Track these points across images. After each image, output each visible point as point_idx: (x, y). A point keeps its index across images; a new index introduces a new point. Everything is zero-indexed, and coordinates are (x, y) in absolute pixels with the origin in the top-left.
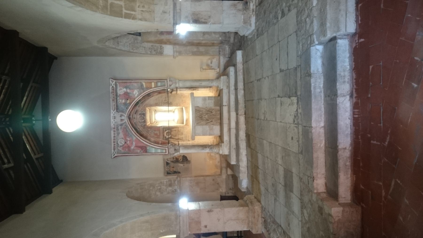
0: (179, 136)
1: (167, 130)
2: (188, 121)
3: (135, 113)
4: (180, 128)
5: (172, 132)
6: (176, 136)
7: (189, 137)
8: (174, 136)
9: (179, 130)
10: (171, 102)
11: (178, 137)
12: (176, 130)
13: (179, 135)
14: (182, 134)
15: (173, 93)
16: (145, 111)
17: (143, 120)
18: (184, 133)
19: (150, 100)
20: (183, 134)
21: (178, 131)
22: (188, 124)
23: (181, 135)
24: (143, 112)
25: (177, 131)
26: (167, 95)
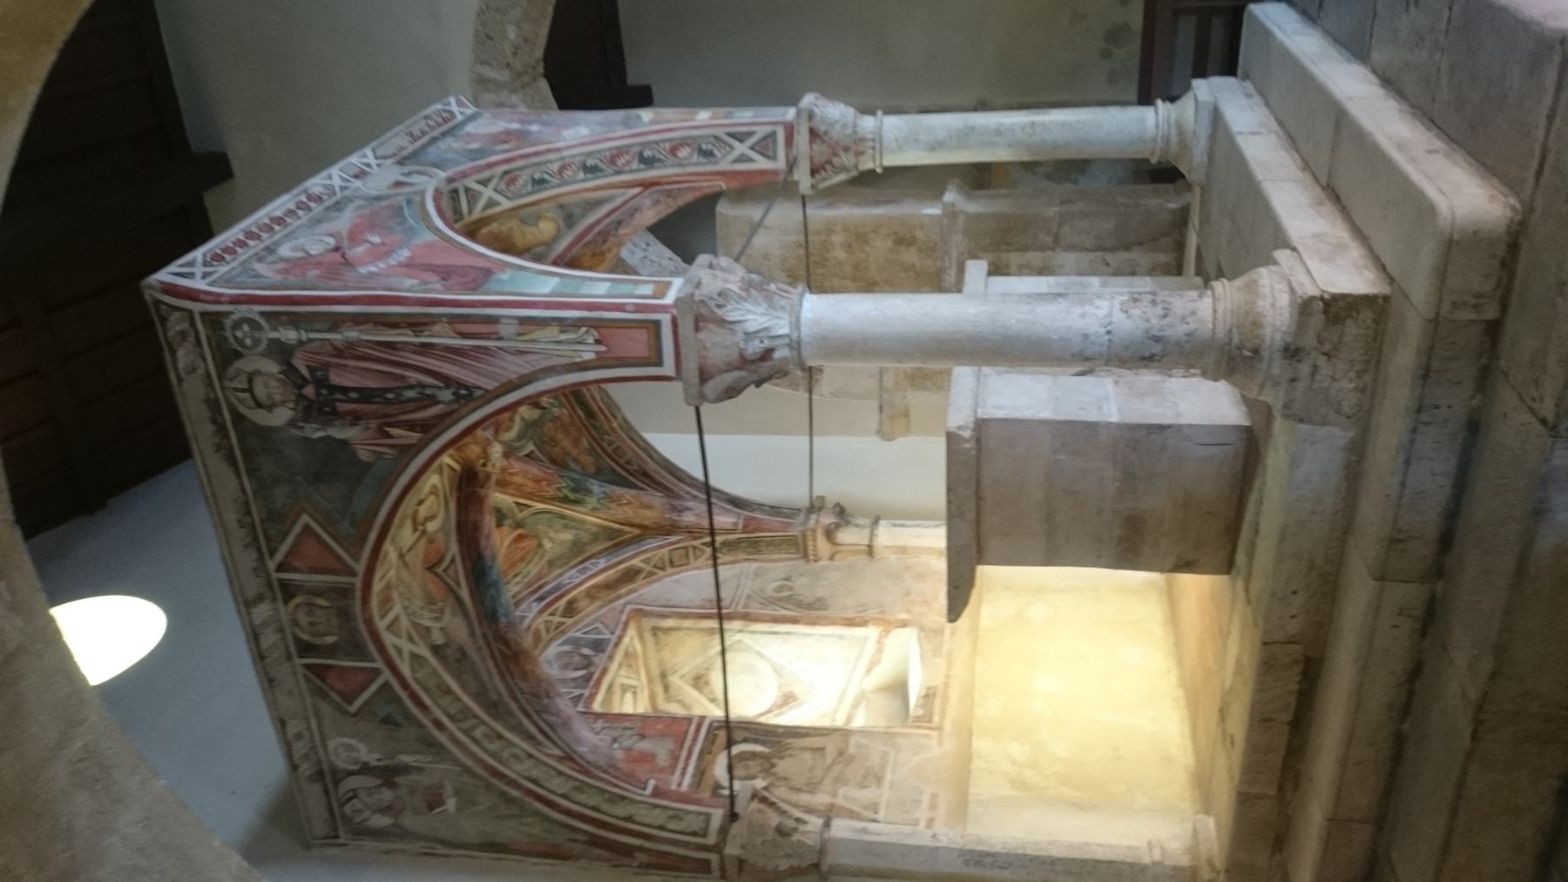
0: (842, 791)
1: (745, 740)
2: (937, 702)
3: (541, 599)
4: (864, 741)
5: (781, 758)
6: (812, 788)
7: (933, 807)
8: (799, 790)
9: (852, 750)
10: (820, 600)
11: (834, 795)
12: (822, 750)
13: (840, 780)
14: (875, 777)
15: (846, 536)
16: (618, 632)
17: (577, 669)
18: (888, 776)
19: (677, 582)
20: (879, 780)
21: (841, 754)
22: (936, 718)
23: (863, 786)
24: (600, 633)
25: (830, 756)
26: (806, 395)
